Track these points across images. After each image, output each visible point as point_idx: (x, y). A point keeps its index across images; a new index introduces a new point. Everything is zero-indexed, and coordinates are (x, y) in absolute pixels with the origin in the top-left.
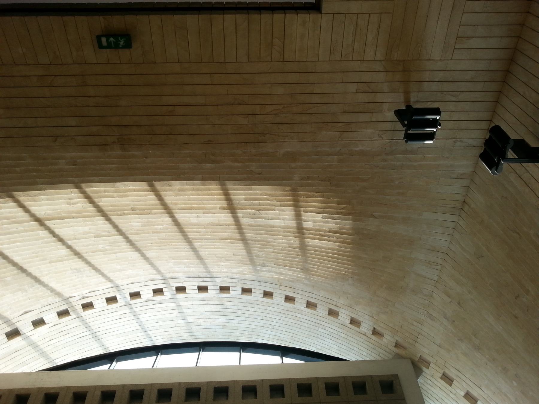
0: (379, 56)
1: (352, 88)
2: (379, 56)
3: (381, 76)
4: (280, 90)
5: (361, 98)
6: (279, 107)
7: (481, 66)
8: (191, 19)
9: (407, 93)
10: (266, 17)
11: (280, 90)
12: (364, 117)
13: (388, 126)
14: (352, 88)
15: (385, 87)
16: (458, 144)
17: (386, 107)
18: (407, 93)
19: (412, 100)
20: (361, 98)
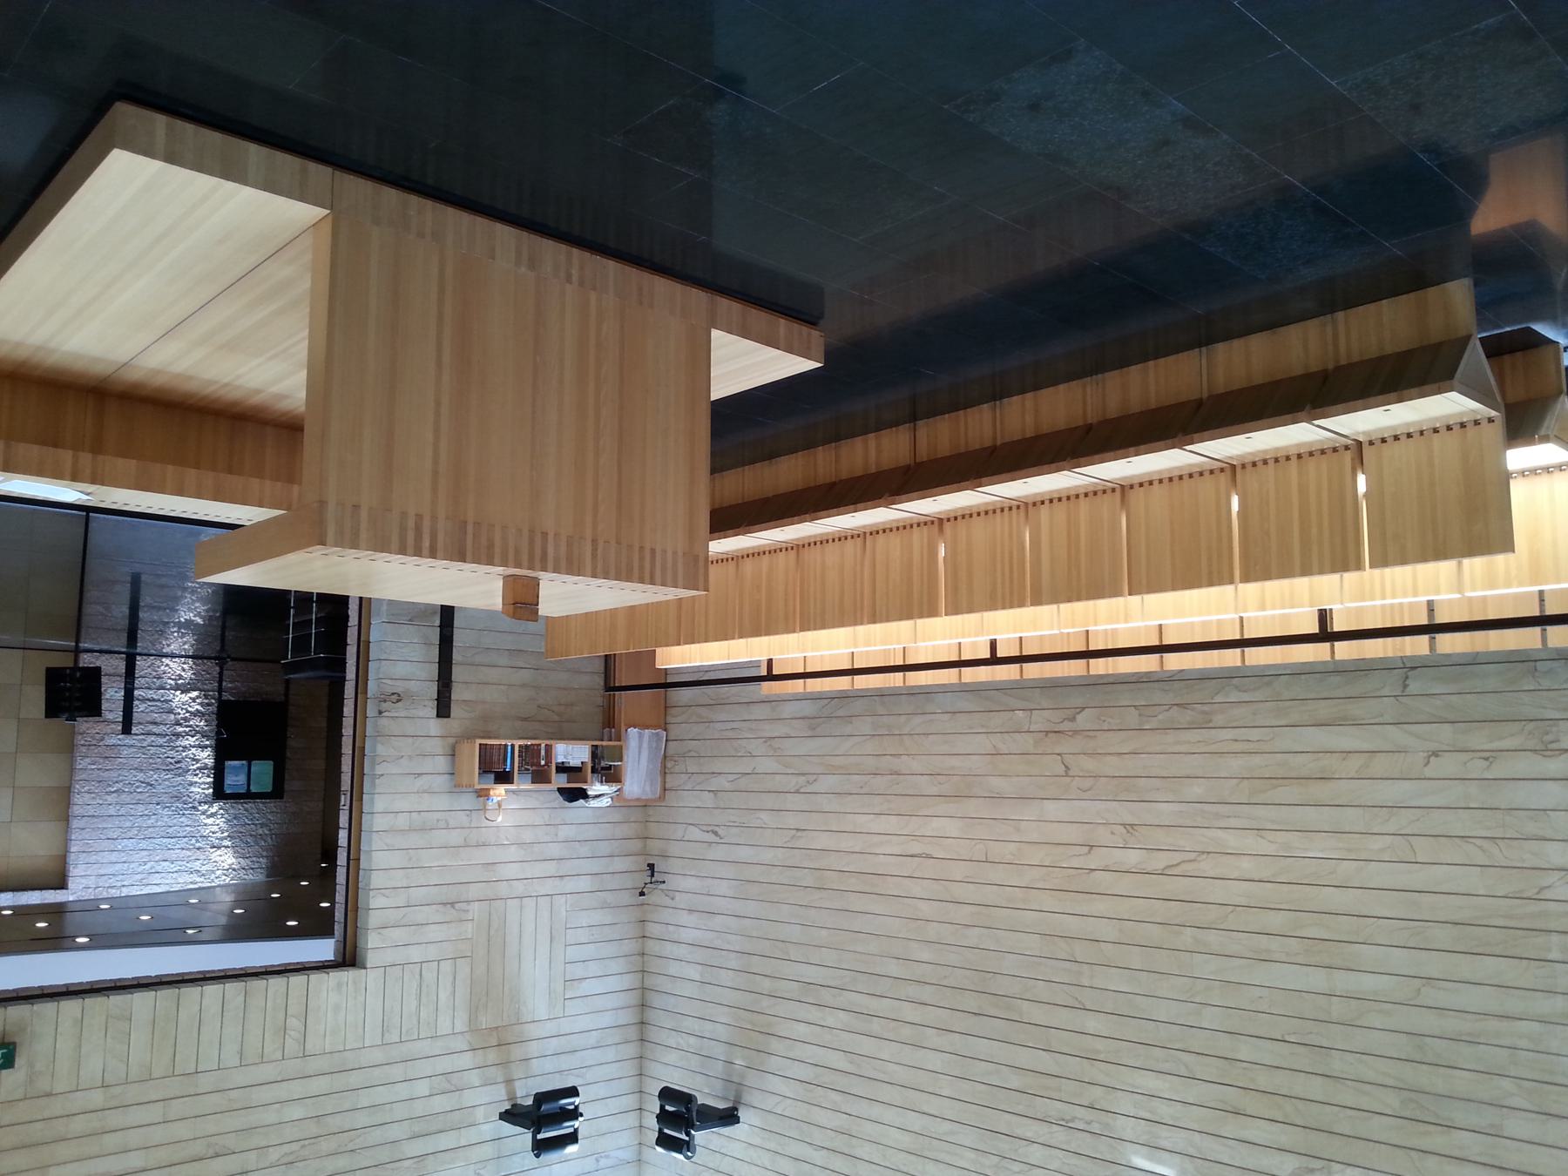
0: (459, 1027)
1: (422, 1088)
2: (459, 1027)
3: (467, 1060)
4: (296, 1112)
5: (440, 1103)
6: (295, 1147)
7: (607, 1019)
8: (141, 999)
9: (509, 1082)
10: (276, 983)
11: (296, 1112)
12: (446, 1141)
13: (487, 1151)
14: (422, 1088)
15: (474, 1078)
16: (603, 1162)
17: (480, 1114)
18: (509, 1082)
19: (519, 1094)
20: (440, 1103)
